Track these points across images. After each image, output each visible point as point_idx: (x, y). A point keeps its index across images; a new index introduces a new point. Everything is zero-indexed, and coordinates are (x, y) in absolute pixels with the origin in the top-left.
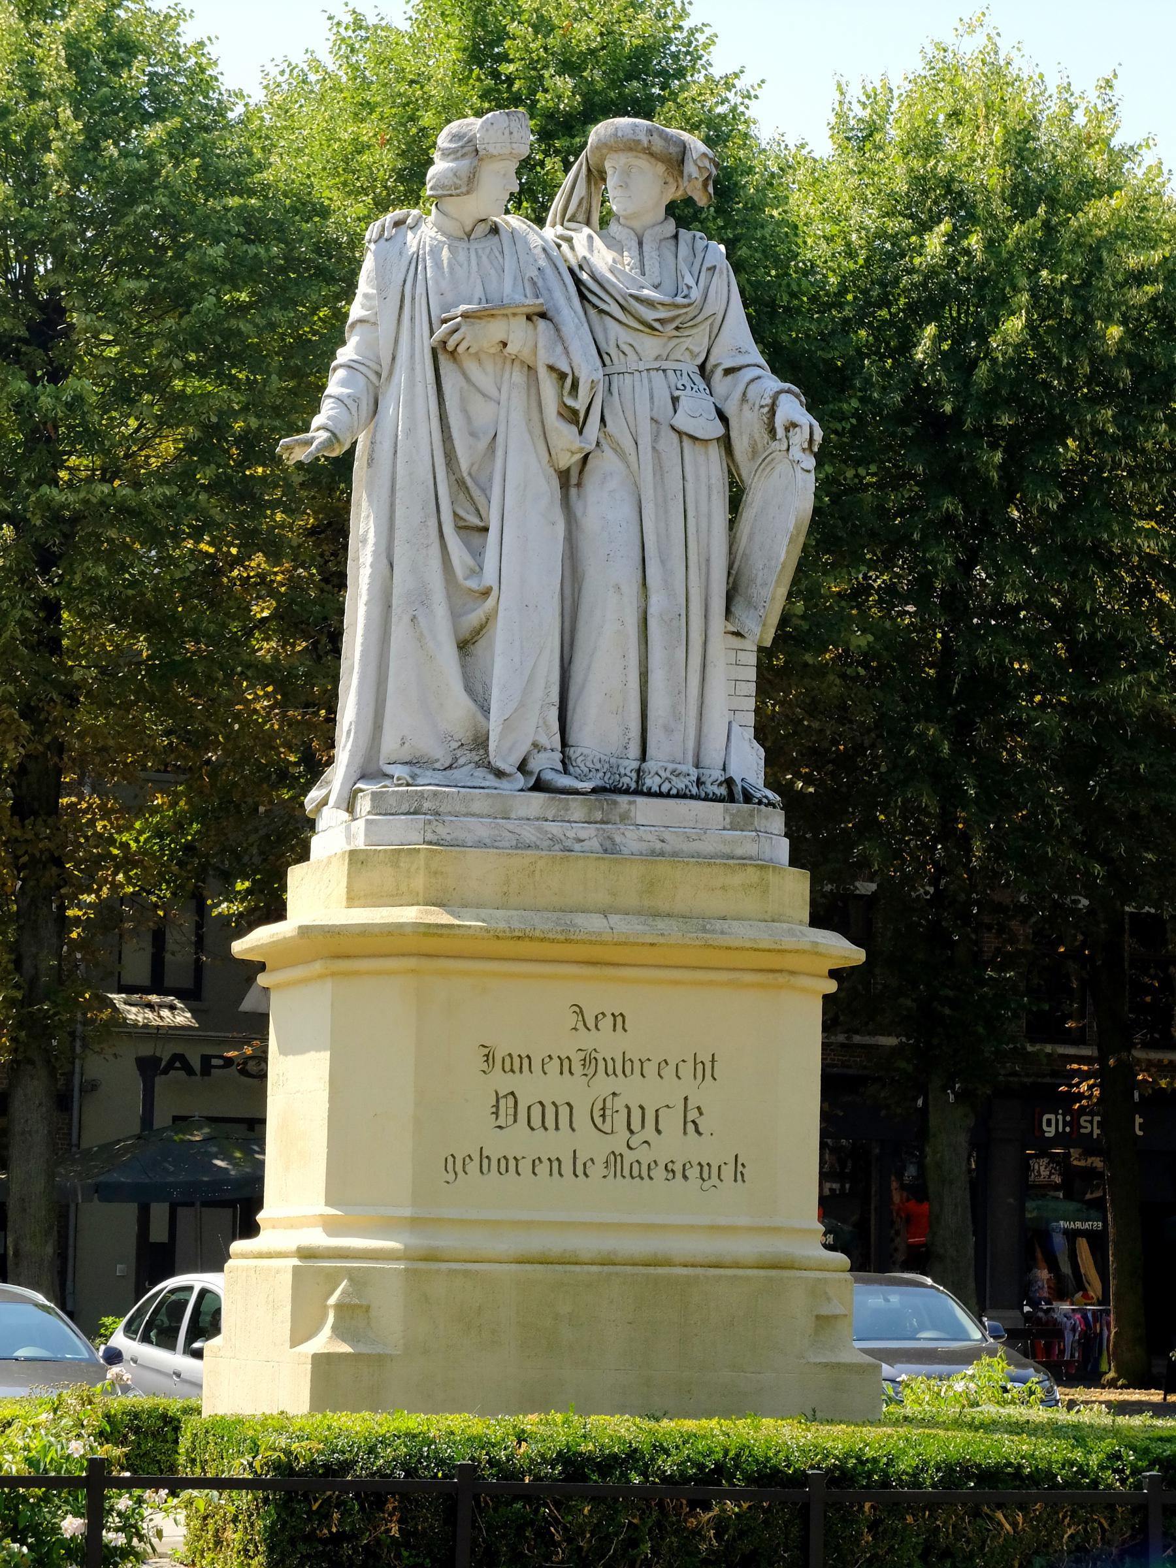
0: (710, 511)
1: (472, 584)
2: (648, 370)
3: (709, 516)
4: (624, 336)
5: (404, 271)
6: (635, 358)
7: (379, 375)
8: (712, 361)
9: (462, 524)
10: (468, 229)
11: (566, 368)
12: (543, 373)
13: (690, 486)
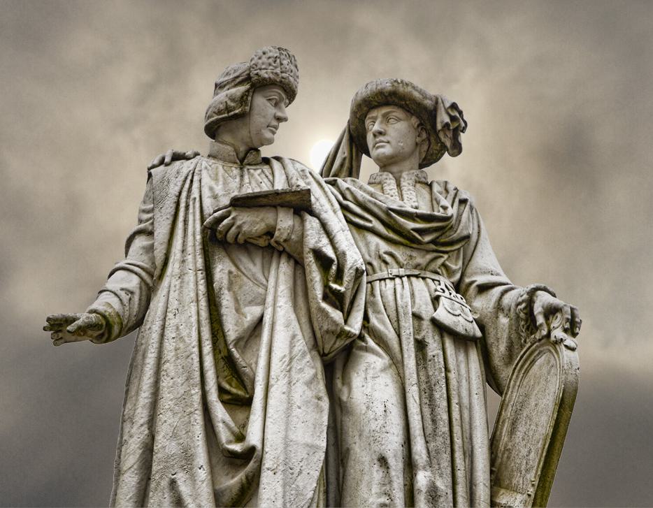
0: (470, 404)
1: (237, 447)
2: (409, 276)
3: (470, 409)
4: (384, 247)
5: (179, 184)
6: (395, 265)
7: (151, 275)
8: (467, 280)
9: (226, 397)
10: (241, 155)
11: (330, 252)
12: (310, 259)
13: (452, 376)
